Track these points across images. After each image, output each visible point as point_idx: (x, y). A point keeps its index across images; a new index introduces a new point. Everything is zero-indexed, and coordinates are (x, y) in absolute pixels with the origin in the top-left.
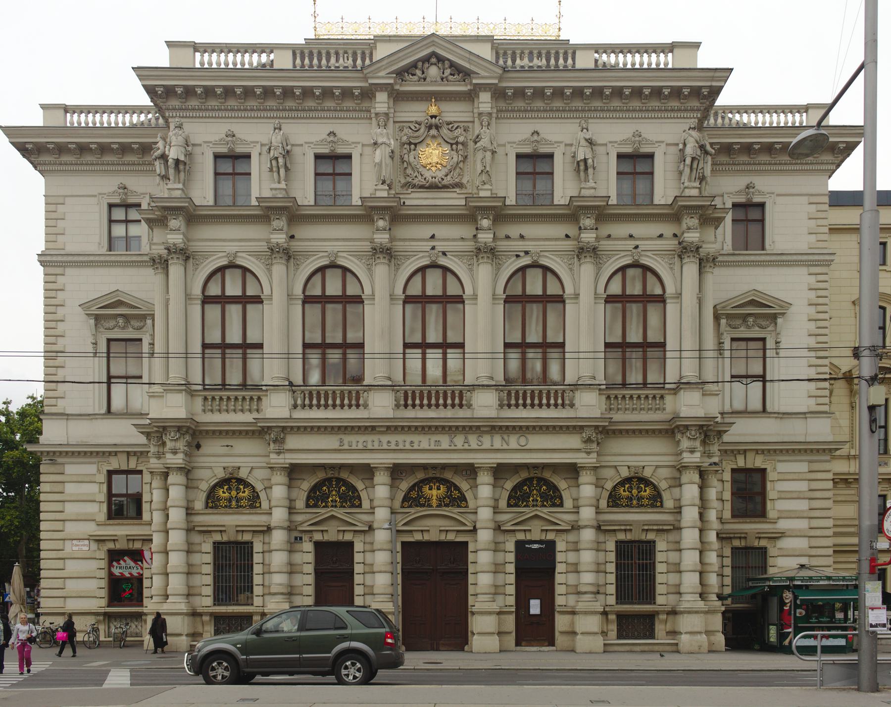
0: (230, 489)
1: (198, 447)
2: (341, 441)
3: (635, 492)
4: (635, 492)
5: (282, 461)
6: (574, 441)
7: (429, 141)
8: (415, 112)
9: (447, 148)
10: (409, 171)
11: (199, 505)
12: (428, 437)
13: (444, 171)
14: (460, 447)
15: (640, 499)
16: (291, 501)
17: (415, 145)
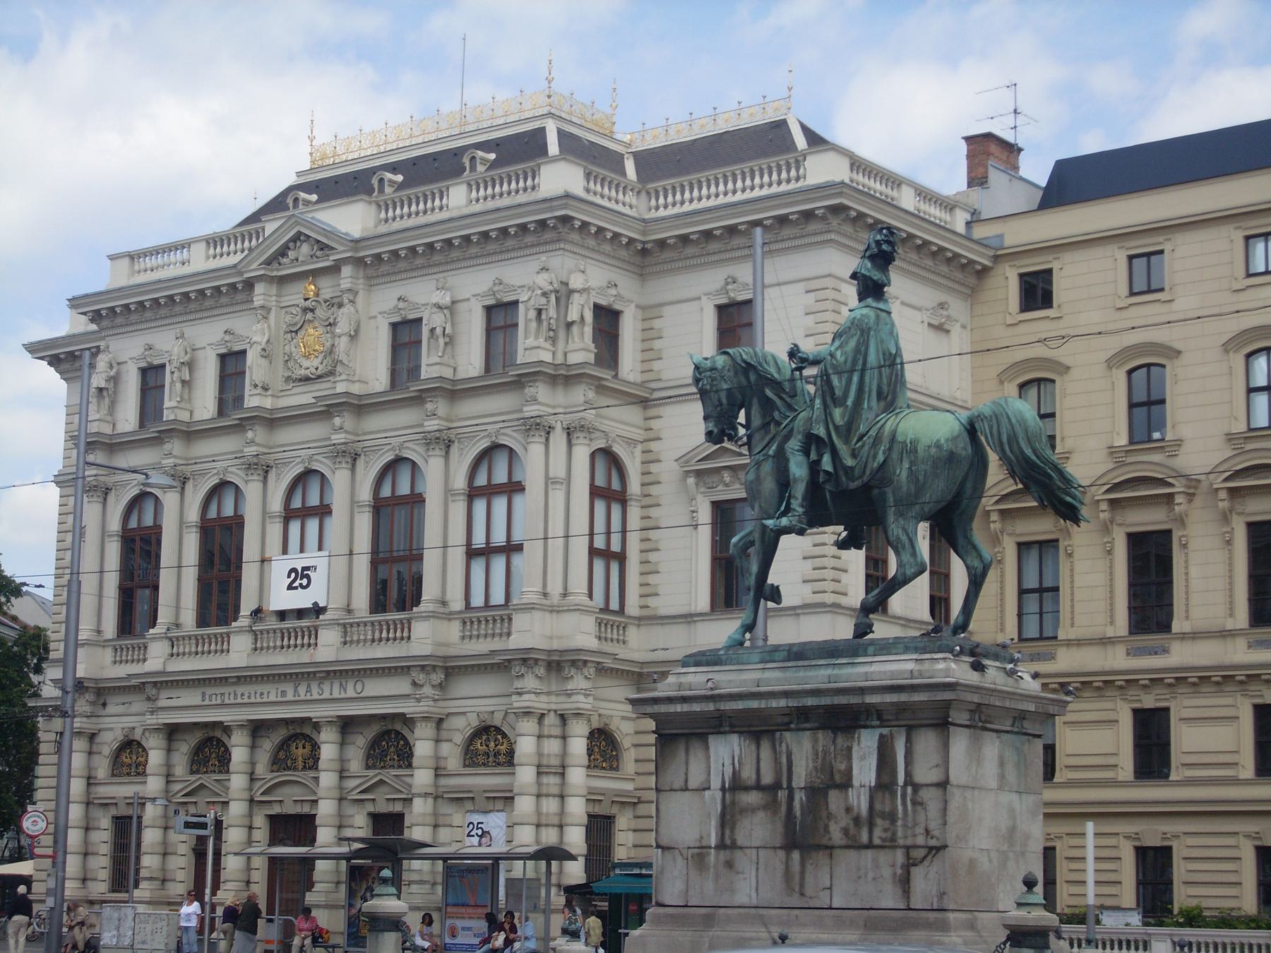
0: (131, 753)
1: (104, 705)
2: (204, 694)
3: (492, 744)
4: (492, 744)
5: (154, 721)
6: (400, 686)
7: (306, 326)
8: (295, 295)
9: (321, 330)
10: (290, 364)
11: (102, 772)
12: (277, 686)
13: (320, 359)
14: (302, 697)
15: (497, 754)
16: (253, 764)
17: (296, 332)
